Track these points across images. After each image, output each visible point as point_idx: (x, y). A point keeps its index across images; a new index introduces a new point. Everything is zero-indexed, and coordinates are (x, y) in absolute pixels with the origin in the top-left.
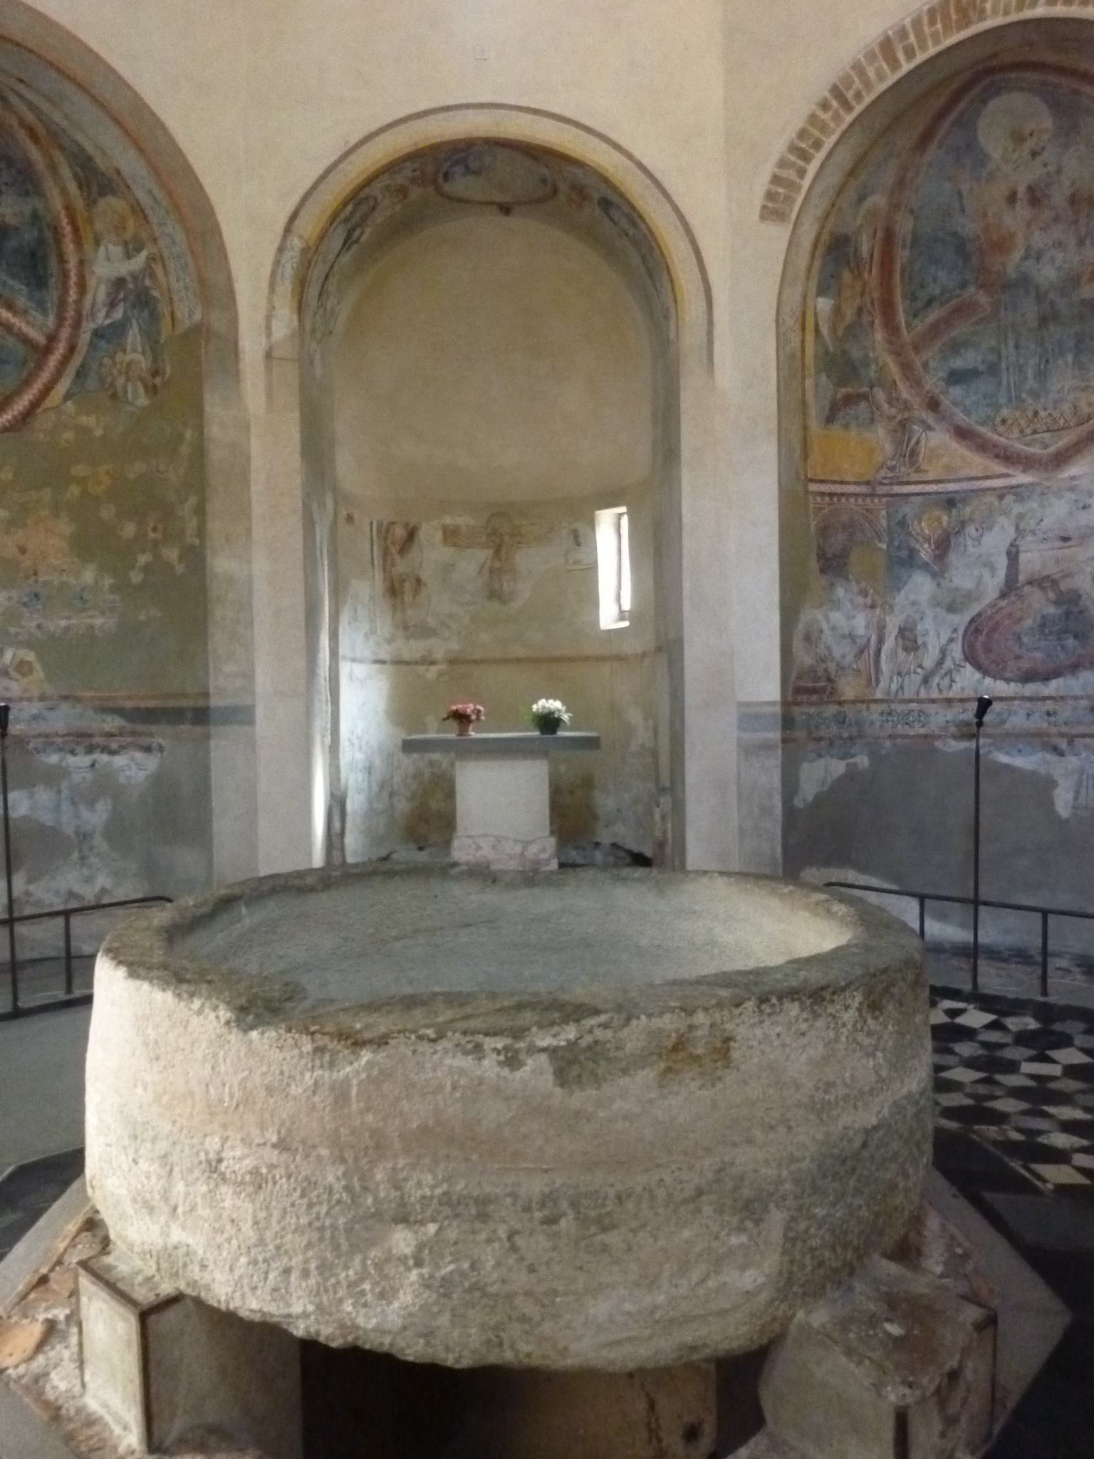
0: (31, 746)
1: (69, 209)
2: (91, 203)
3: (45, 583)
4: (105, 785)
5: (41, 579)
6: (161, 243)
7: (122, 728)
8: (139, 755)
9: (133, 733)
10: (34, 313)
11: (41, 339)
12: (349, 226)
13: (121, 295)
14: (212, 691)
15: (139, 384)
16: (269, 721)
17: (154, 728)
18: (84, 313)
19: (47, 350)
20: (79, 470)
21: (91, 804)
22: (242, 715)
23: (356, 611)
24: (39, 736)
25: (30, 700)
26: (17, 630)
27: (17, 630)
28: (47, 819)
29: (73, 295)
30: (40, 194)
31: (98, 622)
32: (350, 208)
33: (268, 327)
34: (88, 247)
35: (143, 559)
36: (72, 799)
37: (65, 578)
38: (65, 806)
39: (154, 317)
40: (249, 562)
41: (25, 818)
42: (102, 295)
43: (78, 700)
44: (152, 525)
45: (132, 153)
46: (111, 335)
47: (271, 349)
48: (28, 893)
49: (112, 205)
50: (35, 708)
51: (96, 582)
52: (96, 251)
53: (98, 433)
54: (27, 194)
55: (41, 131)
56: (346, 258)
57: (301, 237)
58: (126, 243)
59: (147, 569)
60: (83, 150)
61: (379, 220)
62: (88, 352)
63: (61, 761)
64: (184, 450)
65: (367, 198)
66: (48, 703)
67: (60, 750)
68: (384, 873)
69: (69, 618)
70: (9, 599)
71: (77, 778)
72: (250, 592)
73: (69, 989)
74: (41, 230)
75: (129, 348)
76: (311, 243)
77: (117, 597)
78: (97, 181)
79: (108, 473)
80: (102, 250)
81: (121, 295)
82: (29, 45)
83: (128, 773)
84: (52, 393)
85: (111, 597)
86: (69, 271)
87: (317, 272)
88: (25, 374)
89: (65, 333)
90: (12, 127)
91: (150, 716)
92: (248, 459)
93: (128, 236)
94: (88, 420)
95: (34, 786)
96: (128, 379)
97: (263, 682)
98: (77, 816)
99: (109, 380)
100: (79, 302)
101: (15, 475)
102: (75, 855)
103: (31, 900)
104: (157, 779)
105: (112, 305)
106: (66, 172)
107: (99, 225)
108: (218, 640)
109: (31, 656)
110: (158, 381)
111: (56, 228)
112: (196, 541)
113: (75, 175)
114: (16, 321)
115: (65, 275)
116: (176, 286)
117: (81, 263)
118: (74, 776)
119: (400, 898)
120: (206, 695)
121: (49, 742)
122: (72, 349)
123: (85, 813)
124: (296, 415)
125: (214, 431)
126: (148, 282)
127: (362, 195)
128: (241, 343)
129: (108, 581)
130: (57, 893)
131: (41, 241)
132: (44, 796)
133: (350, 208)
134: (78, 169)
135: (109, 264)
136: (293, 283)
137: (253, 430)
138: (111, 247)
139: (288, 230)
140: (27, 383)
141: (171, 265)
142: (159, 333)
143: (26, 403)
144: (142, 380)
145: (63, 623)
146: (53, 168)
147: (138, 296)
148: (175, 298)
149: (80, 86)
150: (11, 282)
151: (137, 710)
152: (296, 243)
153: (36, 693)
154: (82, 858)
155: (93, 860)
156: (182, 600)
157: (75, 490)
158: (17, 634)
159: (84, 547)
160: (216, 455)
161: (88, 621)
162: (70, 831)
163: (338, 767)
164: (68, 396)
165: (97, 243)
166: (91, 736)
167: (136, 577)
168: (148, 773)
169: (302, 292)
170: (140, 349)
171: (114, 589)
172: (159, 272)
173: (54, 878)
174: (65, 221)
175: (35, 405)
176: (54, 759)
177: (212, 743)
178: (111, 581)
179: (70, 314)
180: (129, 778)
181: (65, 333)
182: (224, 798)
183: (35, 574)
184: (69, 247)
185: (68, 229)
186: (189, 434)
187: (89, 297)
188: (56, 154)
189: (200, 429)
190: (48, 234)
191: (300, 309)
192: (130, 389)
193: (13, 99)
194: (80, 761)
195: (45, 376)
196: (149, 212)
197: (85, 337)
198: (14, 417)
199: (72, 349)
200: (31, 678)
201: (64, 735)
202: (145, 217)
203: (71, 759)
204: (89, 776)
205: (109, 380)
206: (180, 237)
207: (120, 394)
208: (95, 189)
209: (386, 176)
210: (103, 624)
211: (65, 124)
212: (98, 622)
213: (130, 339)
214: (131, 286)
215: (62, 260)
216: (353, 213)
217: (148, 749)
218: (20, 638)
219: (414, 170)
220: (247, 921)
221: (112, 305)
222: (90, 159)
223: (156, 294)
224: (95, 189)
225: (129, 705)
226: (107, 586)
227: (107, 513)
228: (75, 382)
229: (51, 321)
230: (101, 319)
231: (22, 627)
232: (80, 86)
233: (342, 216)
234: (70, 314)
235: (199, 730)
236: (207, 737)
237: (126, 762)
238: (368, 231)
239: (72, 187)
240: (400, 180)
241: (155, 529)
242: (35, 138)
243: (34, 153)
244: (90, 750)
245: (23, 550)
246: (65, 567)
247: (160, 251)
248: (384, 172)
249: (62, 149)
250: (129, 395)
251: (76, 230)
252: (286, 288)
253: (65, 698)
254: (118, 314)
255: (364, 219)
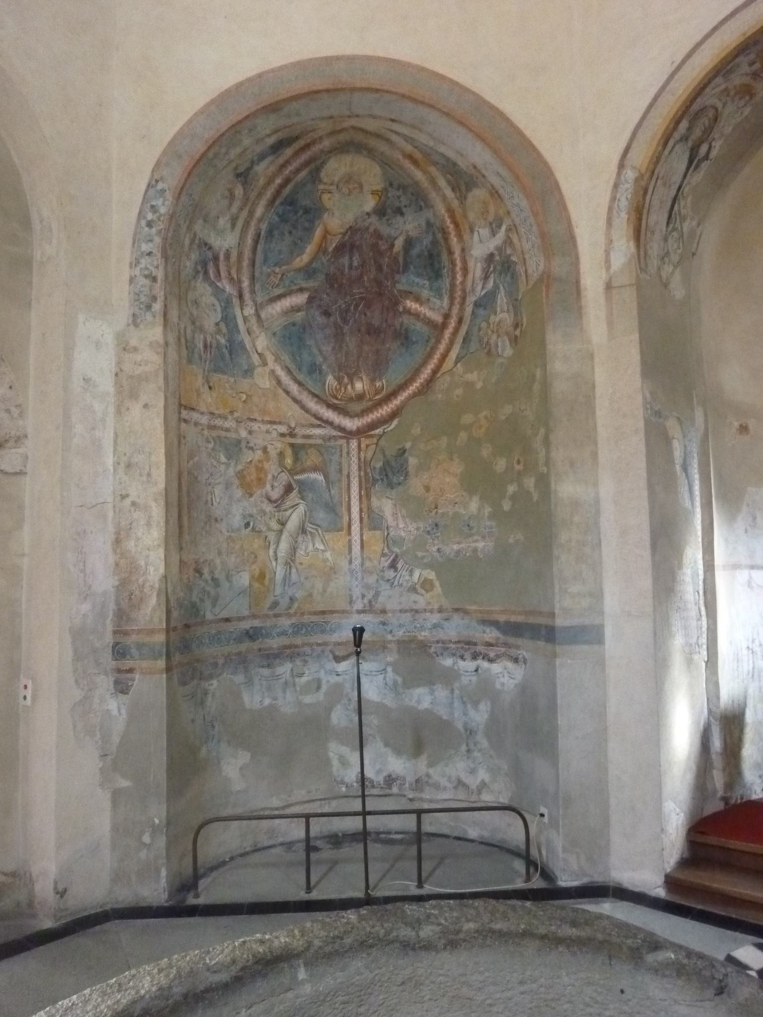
0: (432, 650)
1: (451, 211)
2: (462, 199)
3: (443, 514)
4: (486, 690)
5: (440, 511)
6: (513, 215)
7: (498, 639)
8: (510, 665)
9: (506, 644)
10: (434, 300)
11: (439, 319)
12: (690, 144)
13: (491, 269)
14: (557, 611)
15: (506, 338)
16: (622, 640)
17: (520, 641)
18: (468, 291)
19: (444, 325)
20: (467, 419)
21: (475, 704)
22: (590, 635)
23: (754, 518)
24: (438, 642)
25: (431, 611)
26: (424, 554)
27: (424, 554)
28: (443, 713)
29: (459, 278)
30: (429, 205)
31: (480, 545)
32: (684, 125)
33: (608, 262)
34: (466, 237)
35: (511, 489)
36: (462, 698)
37: (457, 509)
38: (457, 704)
39: (514, 277)
40: (596, 484)
41: (426, 709)
42: (479, 273)
43: (466, 612)
44: (516, 459)
45: (479, 146)
46: (486, 303)
47: (611, 279)
48: (428, 775)
49: (478, 194)
50: (435, 618)
51: (479, 510)
52: (472, 238)
53: (479, 385)
54: (421, 209)
55: (418, 155)
56: (696, 178)
57: (634, 168)
58: (491, 224)
59: (514, 498)
60: (448, 159)
61: (728, 130)
62: (471, 321)
63: (454, 664)
64: (536, 387)
65: (703, 110)
66: (444, 615)
67: (454, 655)
68: (543, 937)
69: (459, 543)
70: (418, 529)
71: (465, 680)
72: (598, 512)
73: (420, 885)
74: (434, 234)
75: (498, 309)
76: (643, 171)
77: (494, 524)
78: (463, 180)
79: (486, 417)
80: (476, 234)
81: (491, 269)
82: (385, 88)
83: (502, 680)
84: (447, 360)
85: (488, 523)
86: (455, 260)
87: (661, 196)
88: (428, 349)
89: (455, 311)
90: (398, 160)
91: (514, 629)
92: (594, 387)
93: (491, 218)
94: (472, 377)
95: (434, 684)
96: (499, 336)
97: (612, 601)
98: (465, 714)
99: (485, 340)
100: (463, 283)
101: (422, 430)
102: (464, 748)
103: (430, 781)
104: (523, 688)
105: (486, 278)
106: (442, 182)
107: (471, 216)
108: (564, 562)
109: (432, 575)
110: (518, 332)
111: (443, 229)
112: (545, 470)
113: (449, 182)
114: (424, 310)
115: (453, 263)
116: (527, 246)
117: (463, 250)
118: (463, 678)
119: (566, 980)
120: (552, 615)
121: (445, 647)
122: (460, 321)
123: (472, 713)
124: (636, 337)
125: (557, 366)
126: (509, 251)
127: (695, 107)
128: (582, 282)
129: (488, 510)
130: (449, 779)
131: (435, 243)
132: (441, 693)
133: (684, 125)
134: (449, 176)
135: (482, 244)
136: (629, 213)
137: (597, 360)
138: (481, 231)
139: (621, 166)
140: (430, 356)
141: (522, 230)
142: (518, 290)
143: (429, 371)
144: (507, 334)
145: (455, 547)
146: (433, 181)
147: (502, 265)
148: (527, 257)
149: (431, 106)
150: (417, 280)
151: (507, 623)
152: (630, 175)
153: (436, 607)
154: (468, 751)
155: (476, 754)
156: (534, 523)
157: (463, 435)
158: (423, 557)
159: (469, 484)
160: (560, 388)
161: (474, 545)
162: (460, 725)
163: (717, 684)
164: (456, 363)
165: (472, 231)
166: (475, 644)
167: (507, 506)
168: (516, 682)
169: (640, 219)
170: (506, 308)
171: (492, 516)
172: (515, 240)
173: (447, 765)
174: (448, 221)
175: (435, 372)
176: (448, 662)
177: (558, 662)
178: (490, 509)
179: (459, 293)
180: (503, 684)
181: (455, 311)
182: (571, 718)
183: (436, 508)
184: (454, 240)
185: (452, 227)
186: (538, 373)
187: (470, 276)
188: (432, 169)
189: (544, 366)
190: (439, 236)
191: (638, 234)
192: (499, 344)
193: (394, 138)
194: (468, 665)
195: (442, 347)
196: (501, 191)
197: (469, 309)
198: (422, 384)
199: (460, 321)
200: (431, 593)
201: (456, 642)
202: (499, 196)
203: (461, 664)
204: (474, 679)
205: (485, 340)
206: (524, 203)
207: (493, 350)
208: (463, 188)
209: (719, 80)
210: (485, 546)
211: (431, 144)
212: (480, 545)
213: (499, 302)
214: (497, 258)
215: (450, 253)
216: (690, 129)
217: (516, 660)
218: (425, 561)
219: (752, 64)
220: (308, 989)
221: (486, 278)
222: (455, 164)
223: (514, 258)
224: (463, 188)
225: (502, 618)
226: (487, 514)
227: (486, 452)
228: (462, 348)
229: (446, 302)
230: (479, 292)
231: (427, 551)
232: (431, 106)
233: (677, 136)
234: (459, 293)
235: (549, 647)
236: (555, 655)
237: (500, 670)
238: (717, 145)
239: (448, 192)
240: (737, 80)
241: (519, 462)
242: (415, 162)
243: (419, 175)
244: (475, 657)
245: (427, 489)
246: (457, 500)
247: (513, 221)
248: (715, 76)
249: (435, 164)
250: (500, 349)
251: (457, 225)
252: (622, 220)
253: (457, 610)
254: (490, 284)
255: (708, 131)
